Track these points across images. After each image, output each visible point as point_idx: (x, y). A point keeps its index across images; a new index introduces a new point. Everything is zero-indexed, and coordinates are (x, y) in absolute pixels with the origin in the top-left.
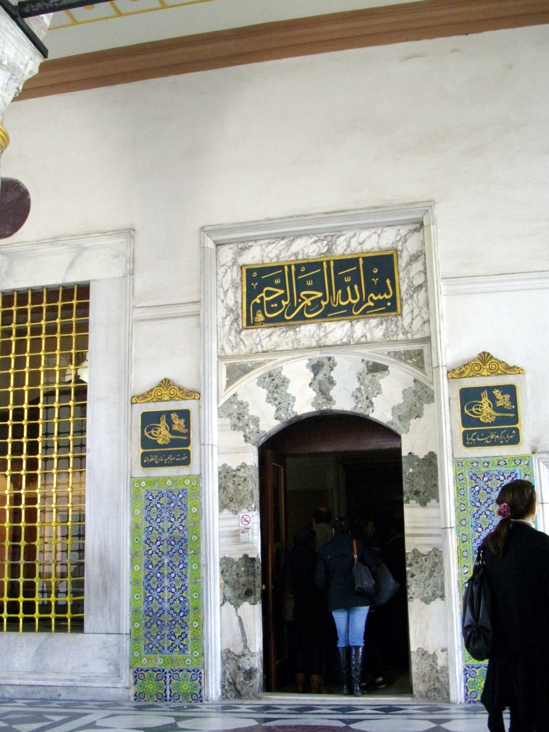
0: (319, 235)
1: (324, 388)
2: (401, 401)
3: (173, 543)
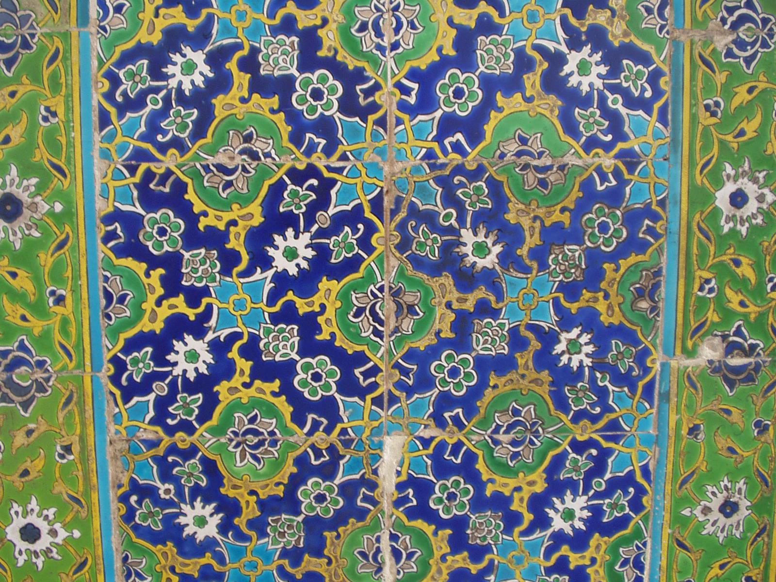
3: (480, 250)
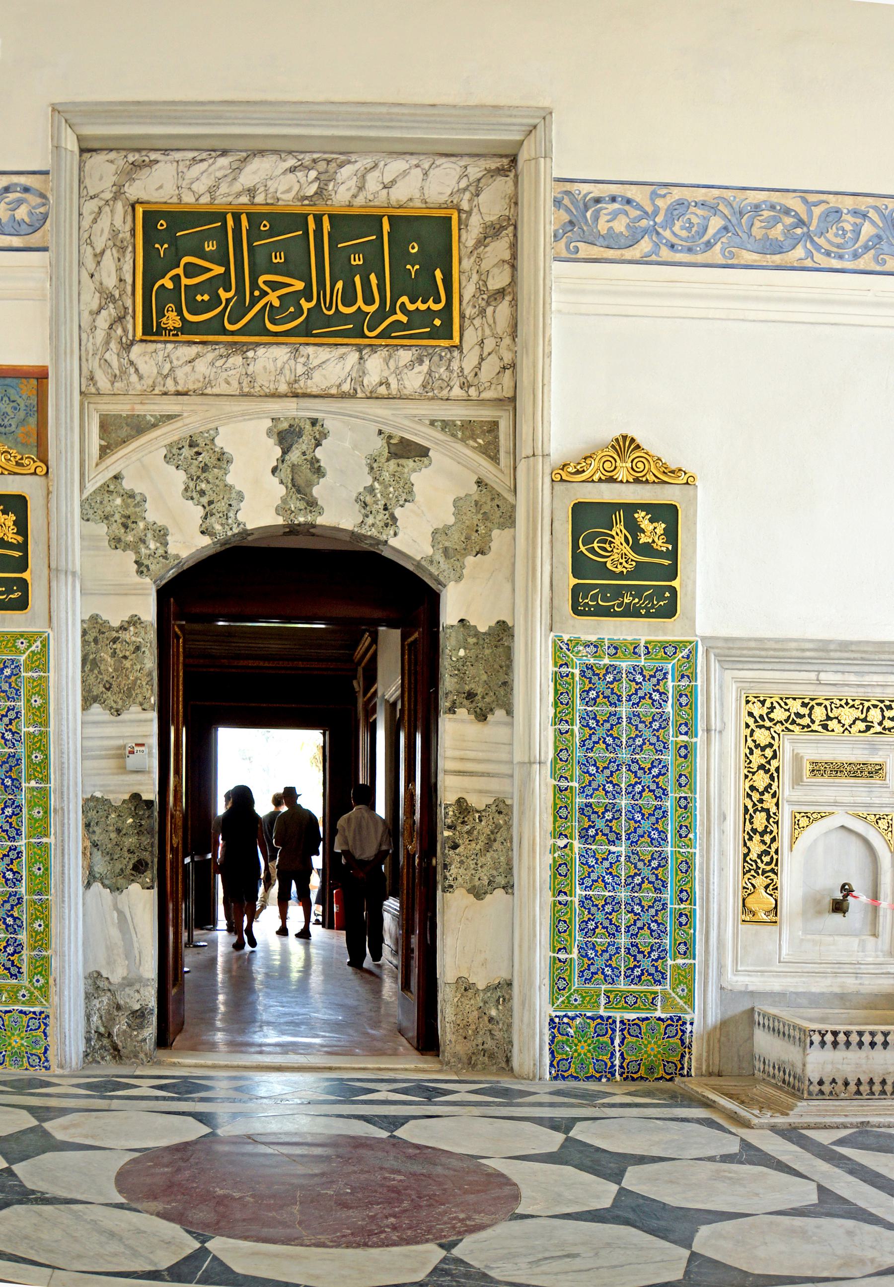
0: (300, 157)
1: (300, 481)
2: (451, 520)
